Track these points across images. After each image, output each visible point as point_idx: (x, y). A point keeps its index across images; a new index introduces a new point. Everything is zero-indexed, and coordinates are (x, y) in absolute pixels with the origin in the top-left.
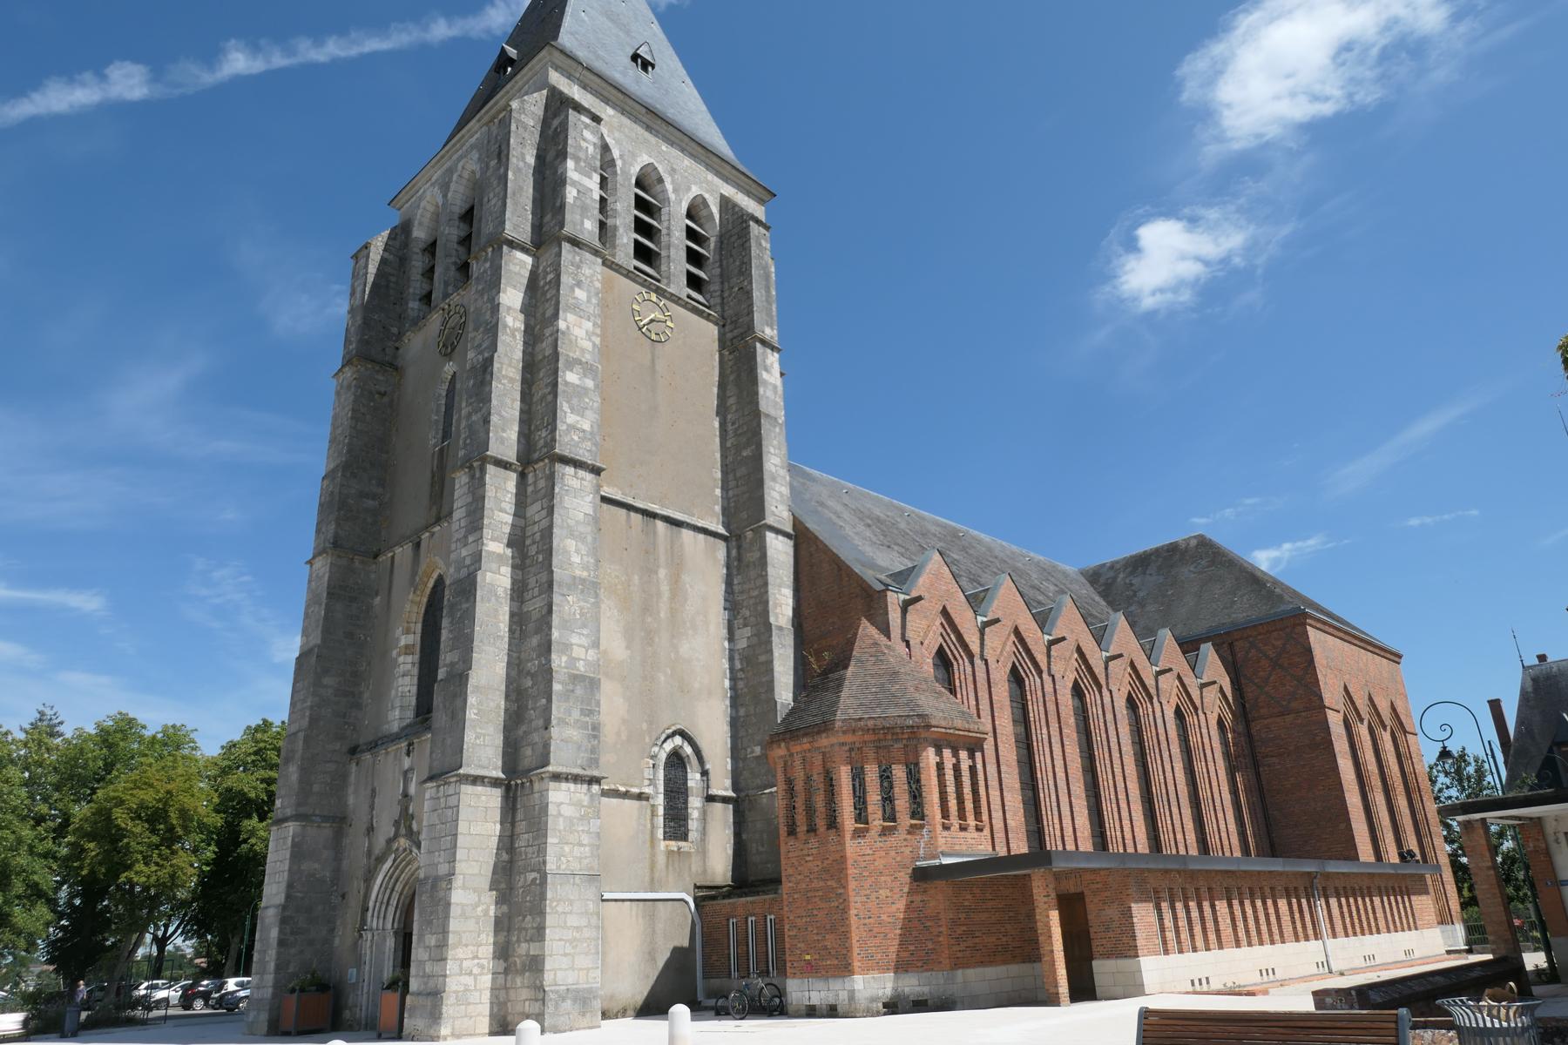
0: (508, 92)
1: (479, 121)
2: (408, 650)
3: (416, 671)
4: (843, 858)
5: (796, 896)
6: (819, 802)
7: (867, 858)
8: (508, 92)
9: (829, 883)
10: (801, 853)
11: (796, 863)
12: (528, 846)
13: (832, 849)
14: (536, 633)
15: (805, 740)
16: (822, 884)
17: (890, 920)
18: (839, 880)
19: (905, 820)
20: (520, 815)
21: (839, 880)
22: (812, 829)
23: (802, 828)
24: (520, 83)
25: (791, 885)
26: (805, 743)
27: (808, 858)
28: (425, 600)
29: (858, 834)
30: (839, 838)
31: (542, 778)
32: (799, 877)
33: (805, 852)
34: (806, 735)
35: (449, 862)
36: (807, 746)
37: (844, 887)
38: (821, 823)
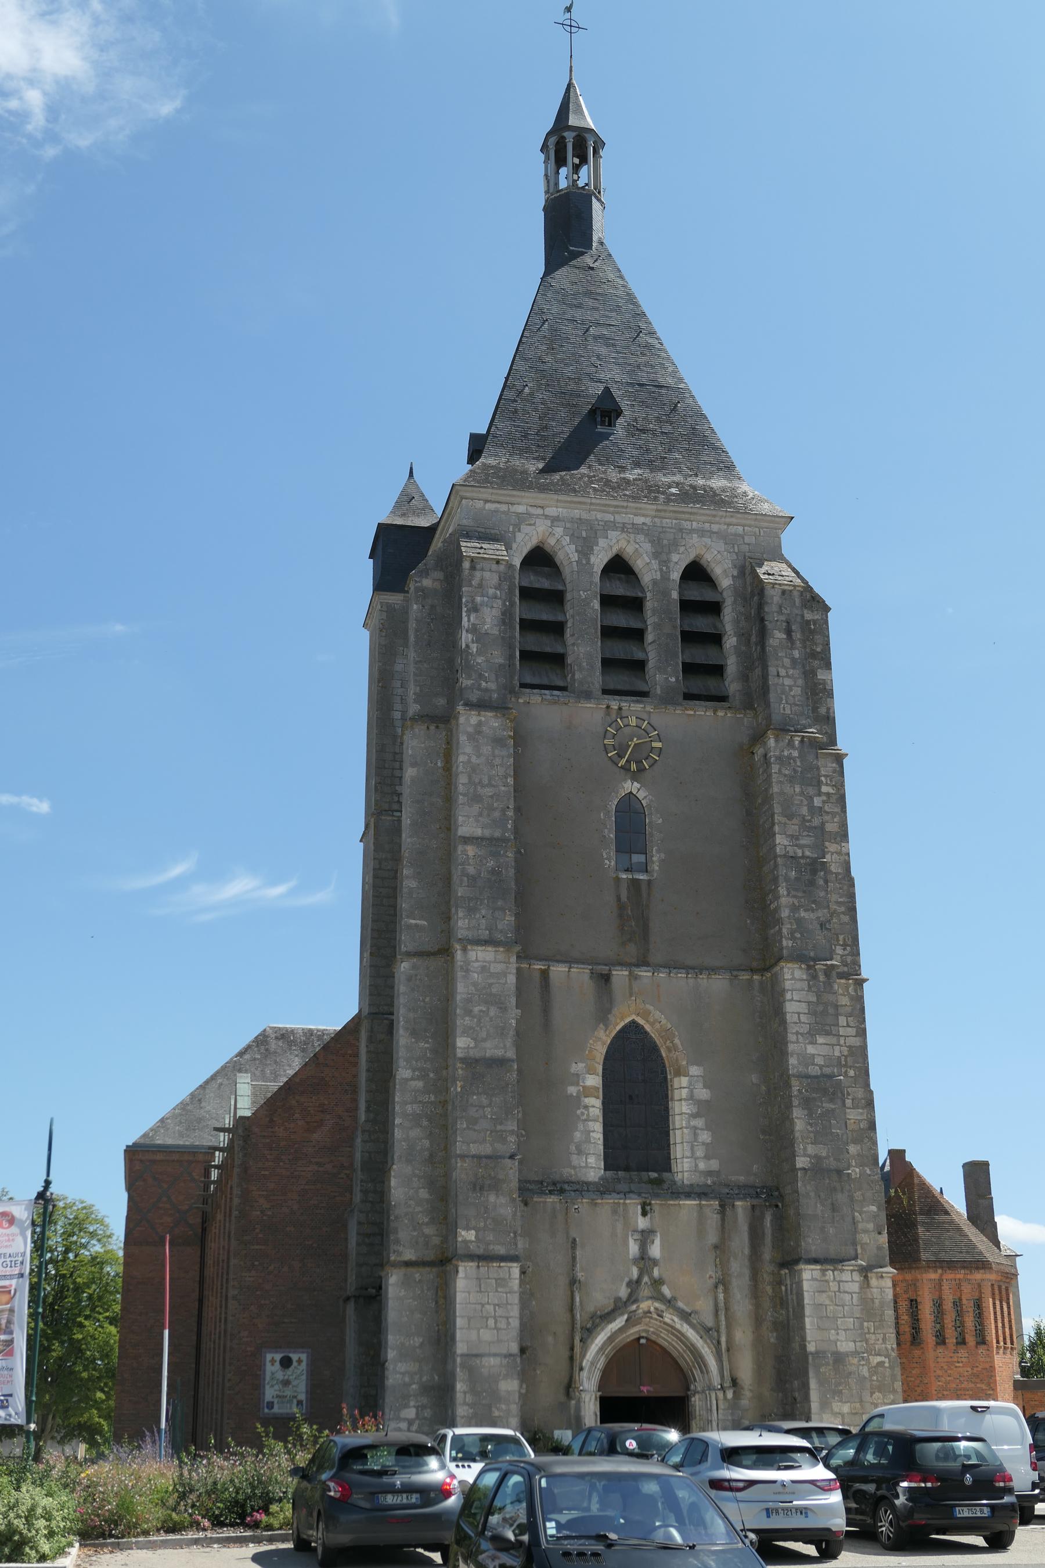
0: (714, 516)
1: (657, 510)
3: (601, 1119)
4: (992, 1368)
6: (970, 1322)
7: (1001, 1369)
8: (714, 516)
9: (978, 1385)
10: (950, 1360)
11: (946, 1367)
12: (869, 1333)
13: (981, 1359)
14: (855, 1142)
15: (963, 1271)
18: (989, 1384)
21: (989, 1384)
22: (962, 1342)
23: (951, 1340)
24: (734, 520)
25: (940, 1383)
26: (960, 1274)
27: (957, 1365)
29: (998, 1353)
30: (988, 1352)
31: (882, 1277)
32: (948, 1378)
33: (956, 1360)
34: (964, 1268)
35: (855, 1342)
36: (961, 1276)
38: (971, 1340)
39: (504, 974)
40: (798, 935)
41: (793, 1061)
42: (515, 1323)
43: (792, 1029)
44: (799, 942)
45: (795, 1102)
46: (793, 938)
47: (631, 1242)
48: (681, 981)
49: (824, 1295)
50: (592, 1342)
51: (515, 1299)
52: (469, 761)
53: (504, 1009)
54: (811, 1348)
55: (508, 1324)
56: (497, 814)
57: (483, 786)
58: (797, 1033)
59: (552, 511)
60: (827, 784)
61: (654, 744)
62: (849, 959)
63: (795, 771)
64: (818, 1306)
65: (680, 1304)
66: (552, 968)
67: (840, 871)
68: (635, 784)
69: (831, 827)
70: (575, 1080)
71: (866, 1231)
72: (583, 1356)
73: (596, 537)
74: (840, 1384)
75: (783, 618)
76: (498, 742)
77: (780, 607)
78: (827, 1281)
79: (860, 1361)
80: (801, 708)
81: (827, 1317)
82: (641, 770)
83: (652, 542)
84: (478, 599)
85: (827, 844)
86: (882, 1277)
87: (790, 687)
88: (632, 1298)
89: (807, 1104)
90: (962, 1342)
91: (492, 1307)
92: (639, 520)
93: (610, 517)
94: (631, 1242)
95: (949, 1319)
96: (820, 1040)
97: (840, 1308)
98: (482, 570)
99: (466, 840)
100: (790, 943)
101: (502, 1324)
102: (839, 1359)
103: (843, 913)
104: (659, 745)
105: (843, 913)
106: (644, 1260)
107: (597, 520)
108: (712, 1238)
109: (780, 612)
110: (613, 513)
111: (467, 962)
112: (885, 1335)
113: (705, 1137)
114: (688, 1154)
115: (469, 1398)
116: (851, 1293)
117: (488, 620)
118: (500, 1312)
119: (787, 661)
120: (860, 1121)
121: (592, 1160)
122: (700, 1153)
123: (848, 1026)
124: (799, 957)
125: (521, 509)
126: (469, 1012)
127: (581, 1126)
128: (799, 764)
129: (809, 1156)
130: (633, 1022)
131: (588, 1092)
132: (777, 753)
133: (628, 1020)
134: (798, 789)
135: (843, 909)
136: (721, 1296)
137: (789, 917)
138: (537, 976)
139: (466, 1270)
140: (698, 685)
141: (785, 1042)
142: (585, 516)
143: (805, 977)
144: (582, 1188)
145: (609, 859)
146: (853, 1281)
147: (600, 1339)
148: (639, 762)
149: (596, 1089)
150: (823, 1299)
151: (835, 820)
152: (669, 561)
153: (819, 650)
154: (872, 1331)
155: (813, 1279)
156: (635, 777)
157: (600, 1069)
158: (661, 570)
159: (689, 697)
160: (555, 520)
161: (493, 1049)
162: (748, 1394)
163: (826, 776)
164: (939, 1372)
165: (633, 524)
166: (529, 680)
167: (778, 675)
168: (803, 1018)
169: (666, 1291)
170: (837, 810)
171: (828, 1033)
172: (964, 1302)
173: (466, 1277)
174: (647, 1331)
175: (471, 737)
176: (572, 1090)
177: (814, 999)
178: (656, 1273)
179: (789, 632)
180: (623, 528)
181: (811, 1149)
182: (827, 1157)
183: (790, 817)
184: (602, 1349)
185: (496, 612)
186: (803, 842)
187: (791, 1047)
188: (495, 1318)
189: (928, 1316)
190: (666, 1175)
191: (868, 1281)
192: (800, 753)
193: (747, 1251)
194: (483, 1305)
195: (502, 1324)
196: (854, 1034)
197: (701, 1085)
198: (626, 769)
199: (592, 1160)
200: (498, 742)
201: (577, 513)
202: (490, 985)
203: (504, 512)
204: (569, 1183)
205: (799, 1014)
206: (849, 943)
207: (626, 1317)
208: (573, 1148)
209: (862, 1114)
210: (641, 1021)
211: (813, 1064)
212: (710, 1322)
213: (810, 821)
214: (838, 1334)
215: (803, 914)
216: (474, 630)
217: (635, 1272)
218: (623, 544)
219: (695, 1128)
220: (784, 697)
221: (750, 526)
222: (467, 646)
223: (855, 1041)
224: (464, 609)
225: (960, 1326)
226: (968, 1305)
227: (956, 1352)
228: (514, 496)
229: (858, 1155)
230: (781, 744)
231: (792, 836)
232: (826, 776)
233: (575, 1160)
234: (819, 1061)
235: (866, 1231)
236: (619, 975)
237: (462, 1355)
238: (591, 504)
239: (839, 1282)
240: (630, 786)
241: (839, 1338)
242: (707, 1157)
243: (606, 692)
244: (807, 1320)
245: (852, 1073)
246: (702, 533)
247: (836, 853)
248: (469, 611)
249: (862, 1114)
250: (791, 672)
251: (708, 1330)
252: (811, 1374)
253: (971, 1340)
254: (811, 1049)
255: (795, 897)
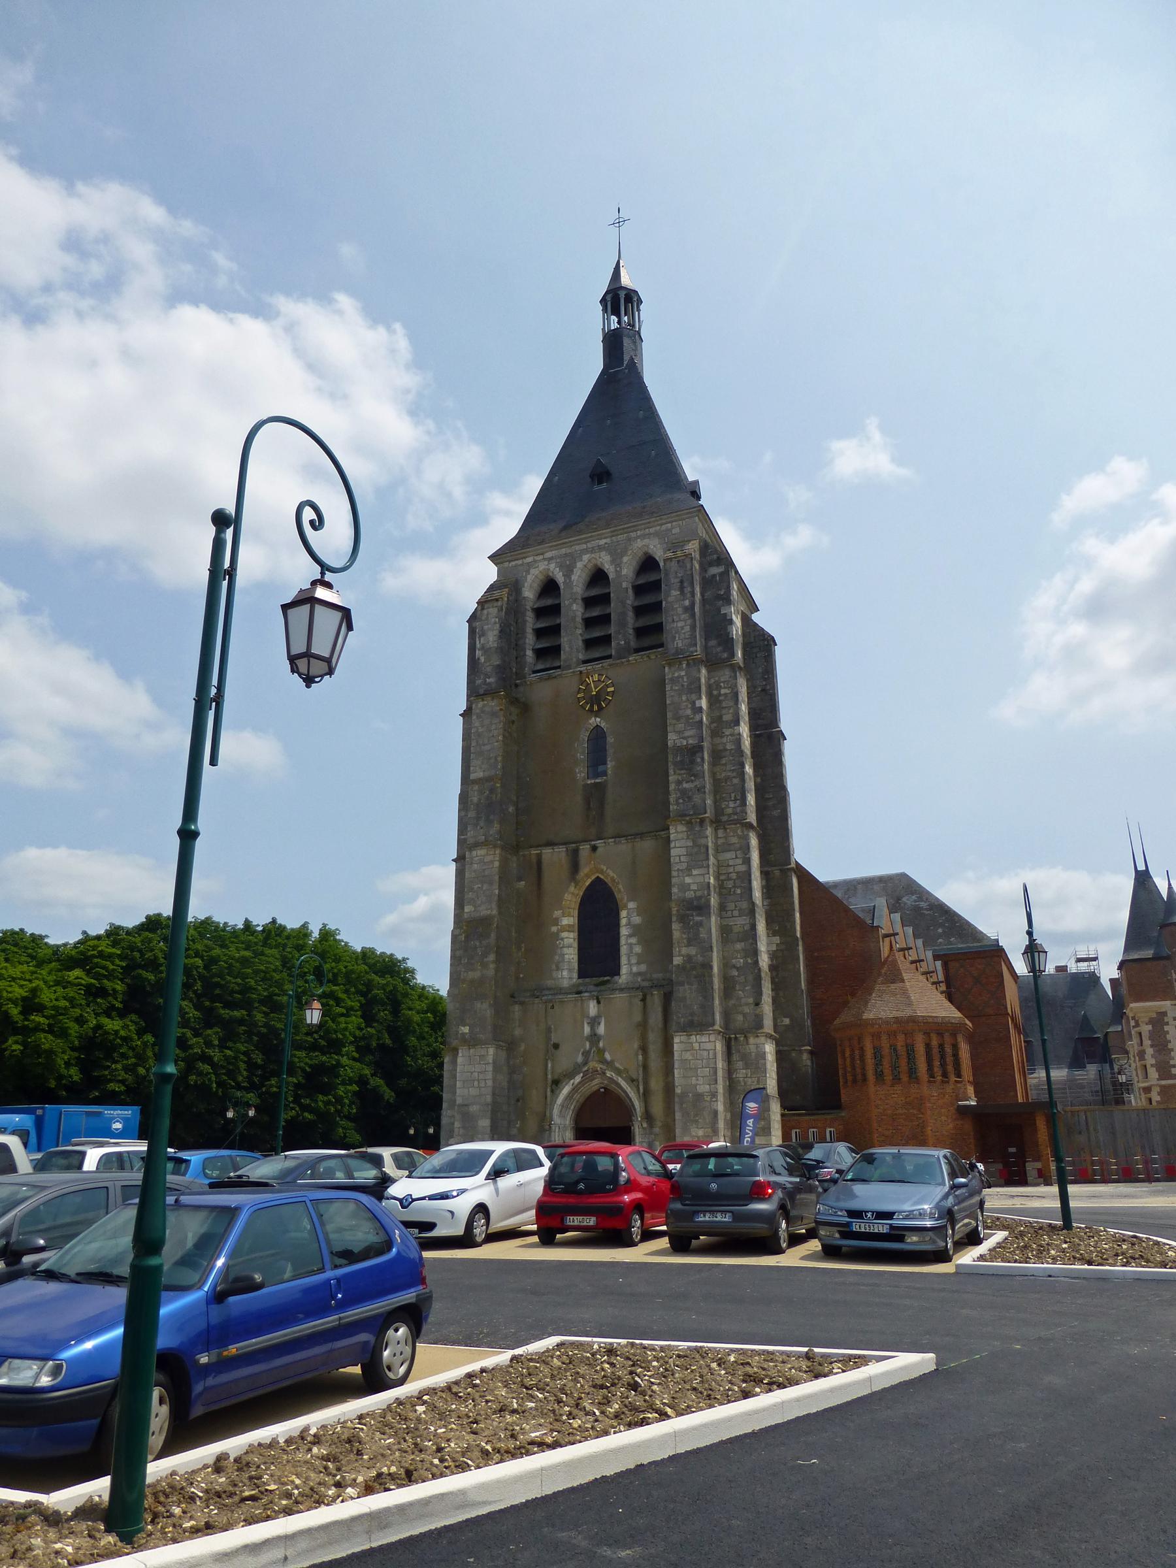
1: (612, 532)
2: (569, 928)
3: (576, 945)
5: (883, 1117)
6: (903, 1063)
9: (911, 1111)
16: (904, 1111)
17: (947, 1134)
19: (953, 1078)
20: (735, 1057)
22: (897, 1079)
23: (888, 1078)
28: (582, 894)
35: (710, 1085)
37: (923, 1114)
39: (492, 862)
40: (681, 801)
41: (675, 890)
42: (490, 1083)
43: (675, 867)
44: (682, 806)
45: (674, 919)
46: (678, 804)
47: (586, 1025)
48: (624, 847)
49: (688, 1053)
50: (560, 1092)
51: (490, 1068)
52: (477, 731)
53: (491, 883)
54: (678, 1091)
55: (486, 1083)
56: (492, 761)
57: (484, 745)
58: (678, 870)
59: (548, 555)
60: (725, 688)
61: (609, 690)
62: (738, 809)
63: (683, 686)
64: (684, 1061)
65: (617, 1065)
66: (543, 851)
67: (733, 747)
68: (598, 719)
69: (727, 717)
70: (556, 922)
71: (747, 1004)
72: (553, 1102)
73: (575, 563)
74: (696, 1115)
75: (678, 580)
76: (494, 714)
77: (676, 573)
78: (692, 1043)
79: (711, 1098)
80: (689, 640)
81: (691, 1069)
82: (601, 708)
83: (611, 554)
84: (486, 627)
85: (724, 730)
86: (757, 1036)
87: (682, 628)
88: (585, 1063)
89: (683, 919)
90: (897, 1079)
91: (476, 1074)
92: (602, 542)
93: (584, 546)
94: (586, 1025)
95: (886, 1063)
96: (695, 872)
97: (700, 1061)
98: (489, 608)
99: (474, 782)
100: (675, 807)
101: (482, 1085)
102: (699, 1097)
103: (734, 777)
104: (612, 689)
105: (734, 777)
106: (594, 1038)
107: (576, 551)
108: (638, 1018)
109: (676, 577)
110: (586, 543)
111: (472, 858)
112: (759, 1078)
113: (638, 949)
114: (626, 963)
115: (462, 1131)
116: (708, 1050)
117: (491, 639)
118: (481, 1077)
119: (680, 610)
120: (744, 925)
121: (565, 973)
122: (634, 961)
123: (736, 857)
124: (682, 815)
125: (529, 560)
126: (471, 890)
127: (559, 951)
128: (685, 680)
129: (682, 956)
130: (598, 877)
131: (563, 929)
132: (670, 676)
133: (593, 877)
134: (684, 698)
135: (735, 774)
136: (640, 1057)
137: (674, 790)
138: (534, 860)
139: (462, 1052)
140: (647, 642)
141: (670, 876)
142: (569, 551)
143: (684, 829)
144: (560, 991)
145: (581, 773)
146: (710, 1041)
147: (566, 1090)
148: (599, 706)
149: (569, 926)
150: (688, 1056)
151: (731, 711)
152: (621, 562)
153: (722, 593)
154: (749, 1075)
155: (681, 1042)
156: (597, 714)
157: (576, 913)
158: (616, 570)
159: (637, 651)
160: (551, 559)
161: (484, 911)
162: (659, 1124)
163: (723, 682)
164: (879, 1102)
165: (599, 546)
166: (540, 667)
167: (673, 621)
168: (683, 859)
169: (608, 1056)
170: (731, 703)
171: (702, 867)
172: (899, 1048)
173: (463, 1056)
174: (603, 1083)
175: (479, 717)
176: (554, 929)
177: (691, 844)
178: (601, 1044)
179: (682, 589)
180: (592, 551)
181: (684, 951)
182: (696, 955)
183: (678, 718)
184: (570, 1096)
185: (496, 632)
186: (687, 734)
187: (674, 881)
188: (478, 1080)
189: (870, 1061)
190: (616, 978)
191: (747, 1040)
192: (686, 673)
193: (661, 1025)
194: (472, 1073)
195: (482, 1085)
196: (741, 863)
197: (635, 914)
198: (591, 710)
199: (565, 973)
200: (494, 714)
201: (563, 551)
202: (484, 870)
203: (522, 565)
204: (549, 989)
205: (680, 856)
206: (739, 798)
207: (582, 1075)
208: (554, 967)
209: (745, 919)
210: (602, 877)
211: (689, 890)
212: (634, 1077)
213: (693, 718)
214: (697, 1080)
215: (685, 785)
216: (482, 648)
217: (588, 1045)
218: (594, 561)
219: (631, 944)
220: (677, 635)
221: (675, 521)
222: (479, 659)
223: (743, 868)
224: (478, 636)
225: (895, 1067)
226: (902, 1051)
227: (892, 1086)
228: (524, 553)
229: (743, 950)
230: (673, 669)
231: (679, 732)
232: (723, 682)
233: (554, 974)
234: (694, 887)
235: (747, 1004)
236: (585, 849)
237: (459, 1105)
238: (570, 542)
239: (700, 1043)
240: (594, 721)
241: (698, 1082)
242: (638, 963)
243: (585, 662)
244: (676, 1072)
245: (739, 891)
246: (643, 537)
247: (730, 735)
248: (480, 637)
249: (745, 919)
250: (683, 617)
251: (633, 1081)
252: (677, 1108)
253: (905, 1078)
254: (688, 880)
255: (679, 774)
